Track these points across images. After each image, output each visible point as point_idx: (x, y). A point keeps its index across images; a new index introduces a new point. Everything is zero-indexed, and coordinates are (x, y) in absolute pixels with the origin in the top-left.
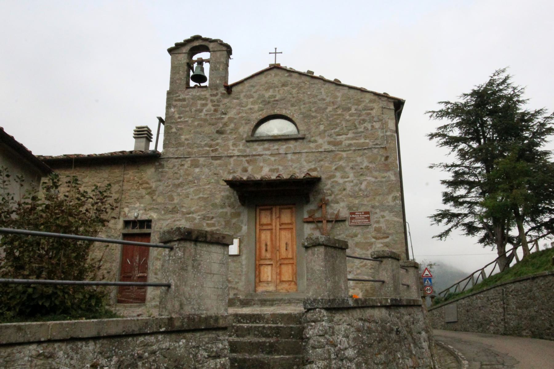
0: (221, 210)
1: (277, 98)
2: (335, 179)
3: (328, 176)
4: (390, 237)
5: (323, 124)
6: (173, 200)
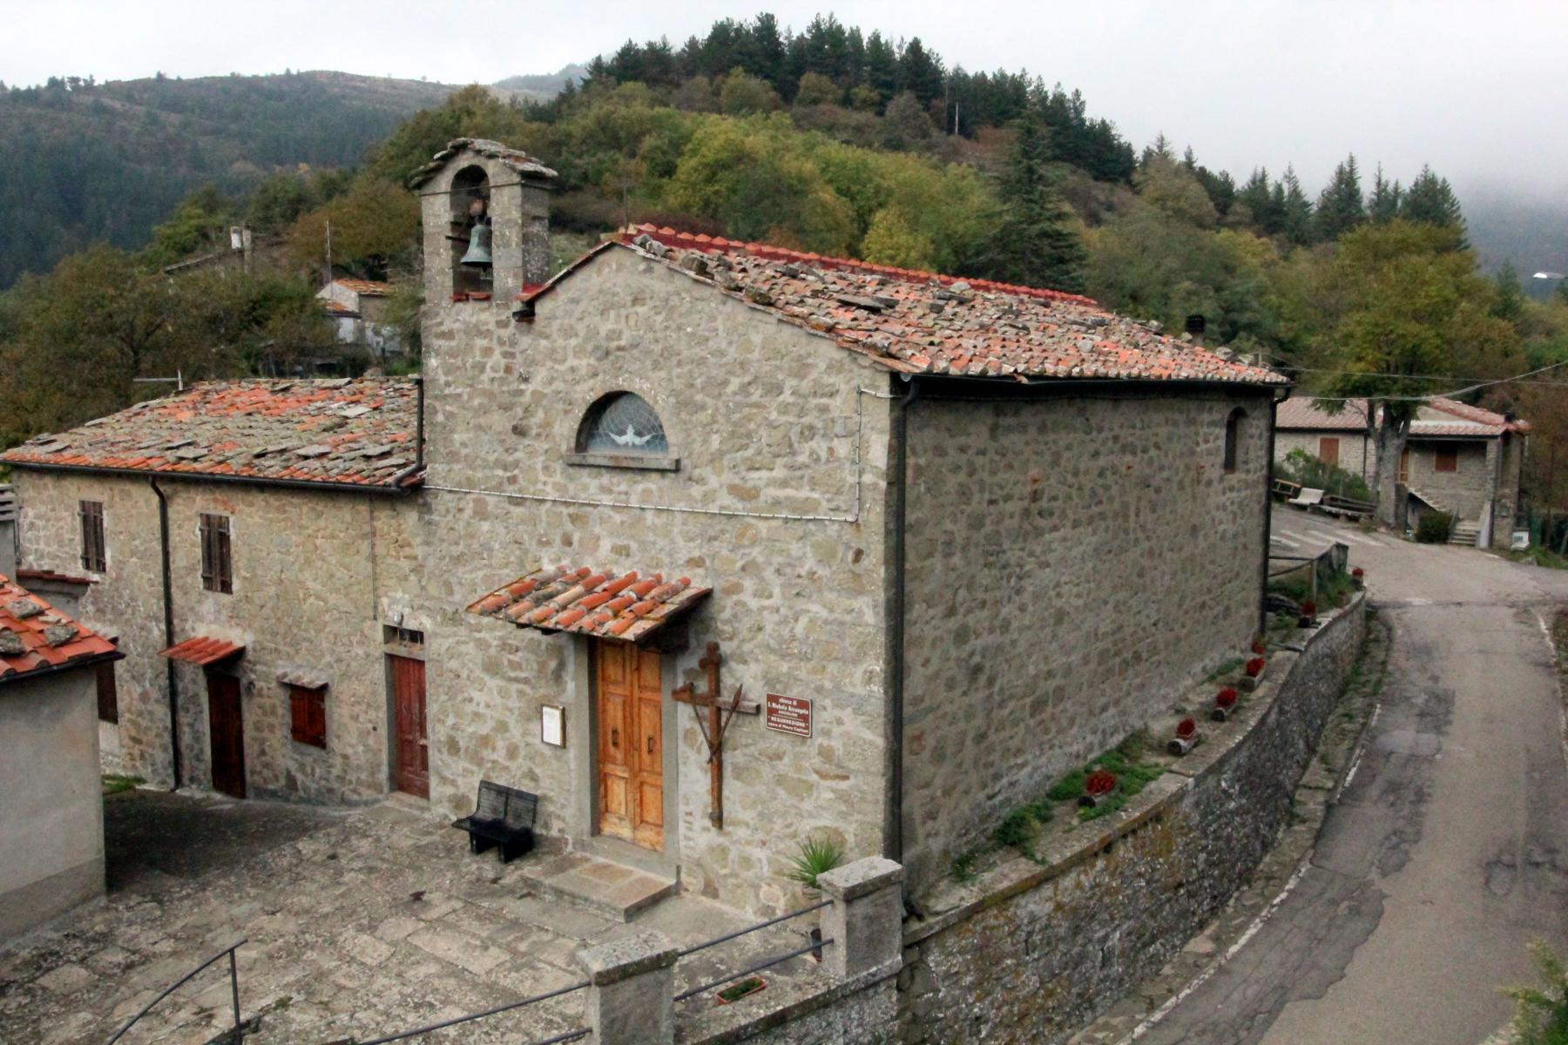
1: (623, 343)
3: (727, 585)
4: (852, 781)
6: (451, 593)
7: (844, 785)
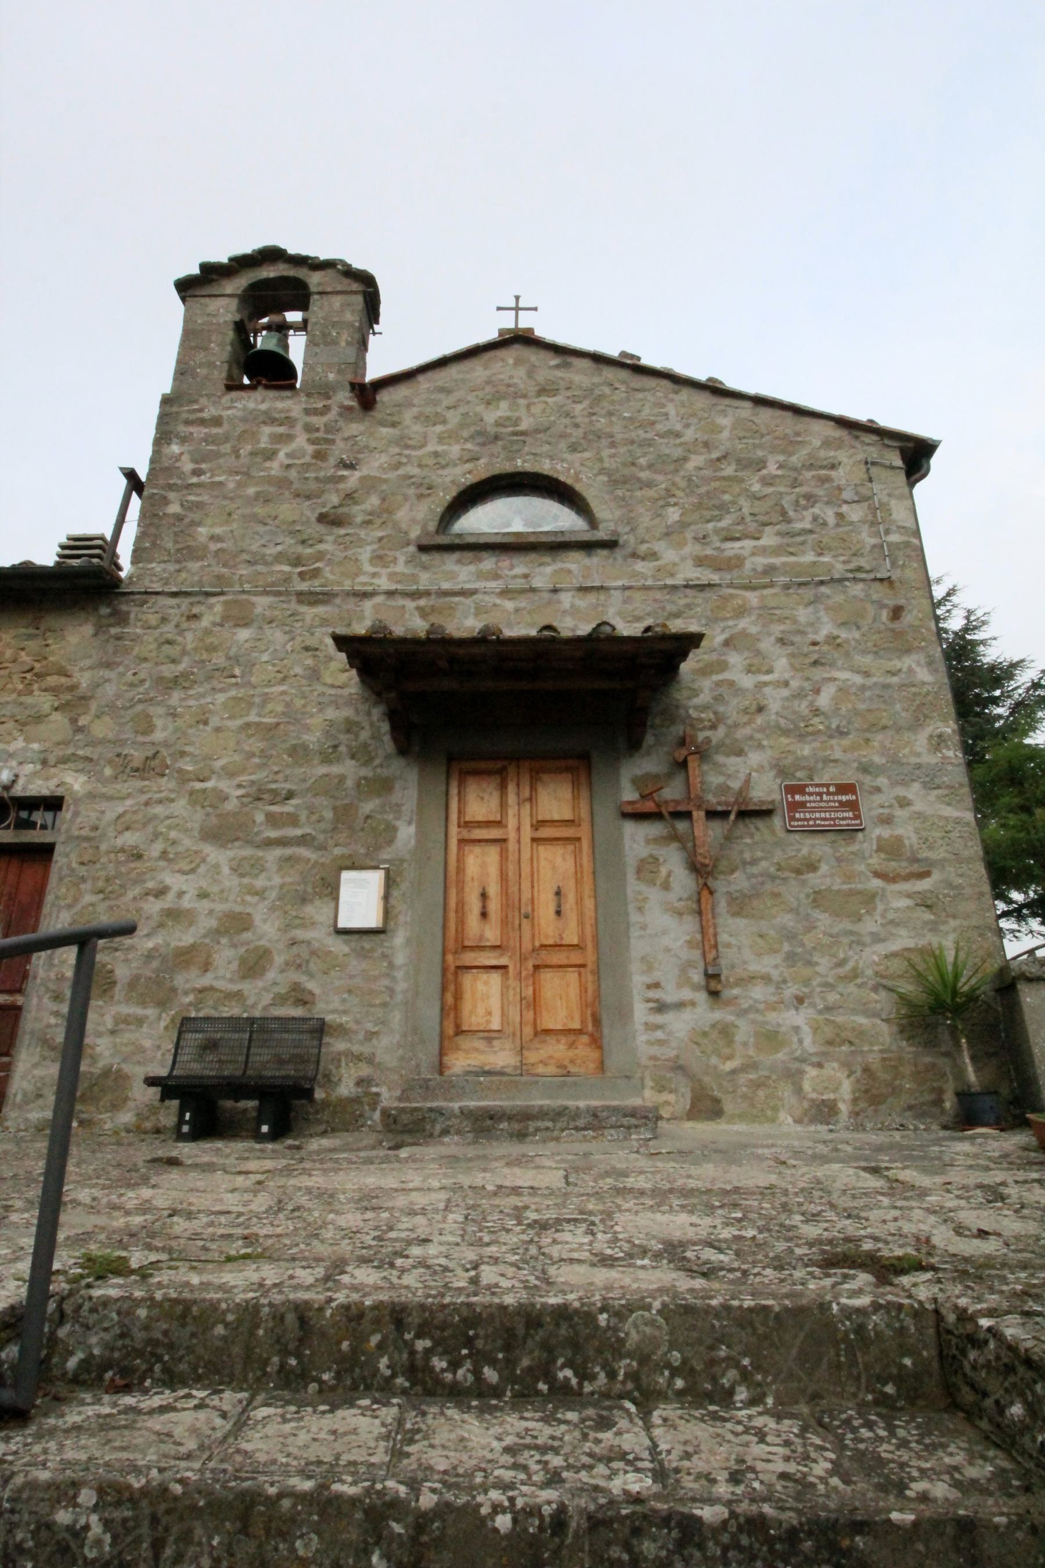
0: (323, 770)
1: (523, 426)
2: (725, 676)
3: (701, 665)
4: (936, 876)
5: (675, 504)
6: (150, 729)
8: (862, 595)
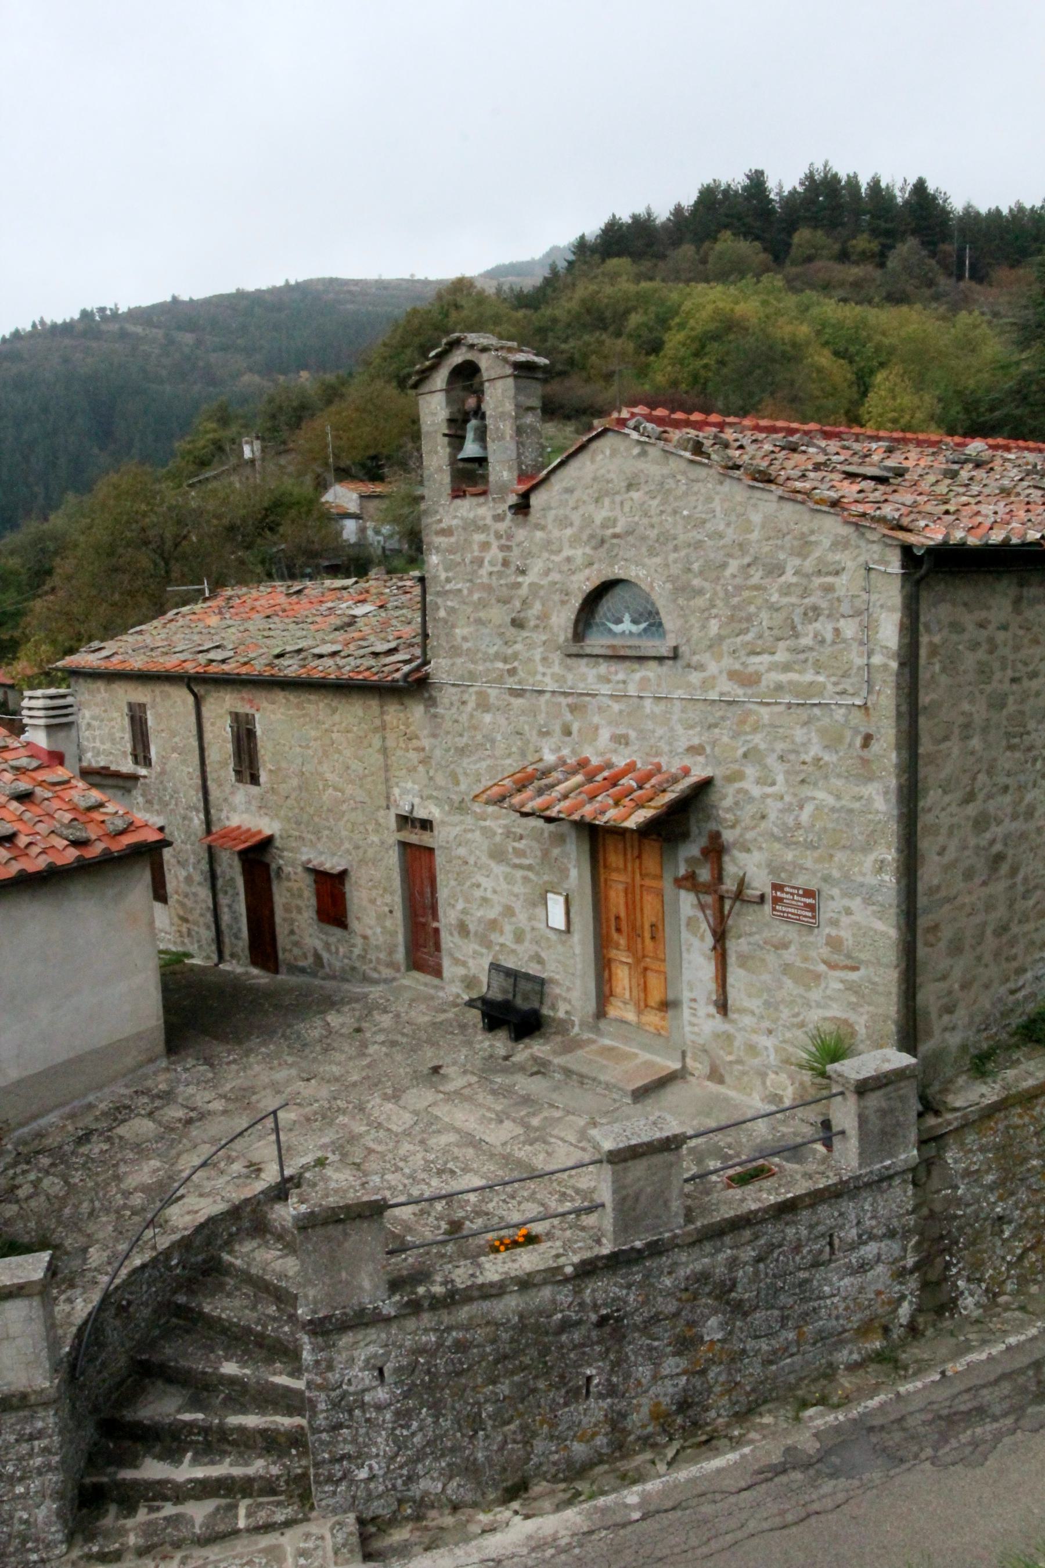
1: (618, 530)
3: (728, 772)
4: (862, 972)
6: (457, 783)
7: (853, 976)
8: (842, 720)
